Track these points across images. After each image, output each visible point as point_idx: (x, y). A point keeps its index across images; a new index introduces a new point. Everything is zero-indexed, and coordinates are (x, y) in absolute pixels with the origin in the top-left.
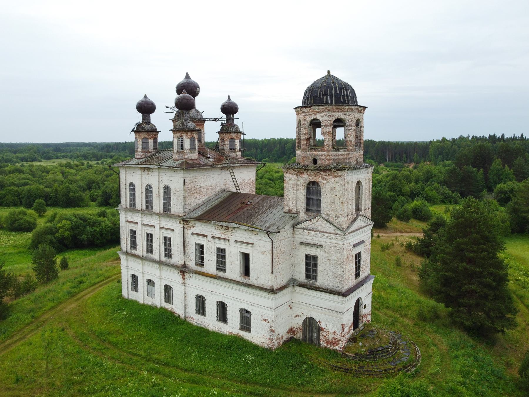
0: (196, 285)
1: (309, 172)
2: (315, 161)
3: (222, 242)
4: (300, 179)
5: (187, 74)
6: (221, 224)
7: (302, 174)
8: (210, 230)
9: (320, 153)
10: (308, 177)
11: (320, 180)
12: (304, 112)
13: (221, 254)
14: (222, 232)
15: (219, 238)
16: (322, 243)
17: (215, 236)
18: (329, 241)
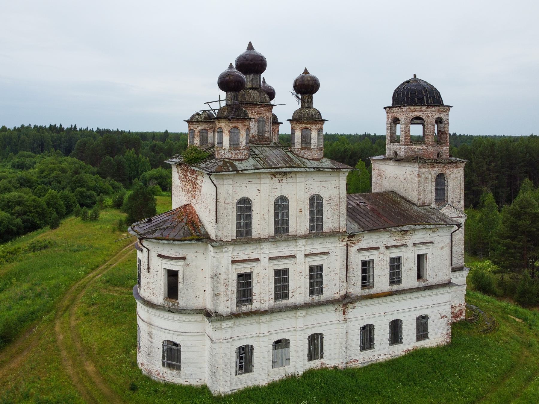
0: (362, 314)
3: (398, 250)
5: (250, 43)
6: (399, 229)
8: (381, 240)
12: (433, 111)
14: (397, 238)
15: (396, 246)
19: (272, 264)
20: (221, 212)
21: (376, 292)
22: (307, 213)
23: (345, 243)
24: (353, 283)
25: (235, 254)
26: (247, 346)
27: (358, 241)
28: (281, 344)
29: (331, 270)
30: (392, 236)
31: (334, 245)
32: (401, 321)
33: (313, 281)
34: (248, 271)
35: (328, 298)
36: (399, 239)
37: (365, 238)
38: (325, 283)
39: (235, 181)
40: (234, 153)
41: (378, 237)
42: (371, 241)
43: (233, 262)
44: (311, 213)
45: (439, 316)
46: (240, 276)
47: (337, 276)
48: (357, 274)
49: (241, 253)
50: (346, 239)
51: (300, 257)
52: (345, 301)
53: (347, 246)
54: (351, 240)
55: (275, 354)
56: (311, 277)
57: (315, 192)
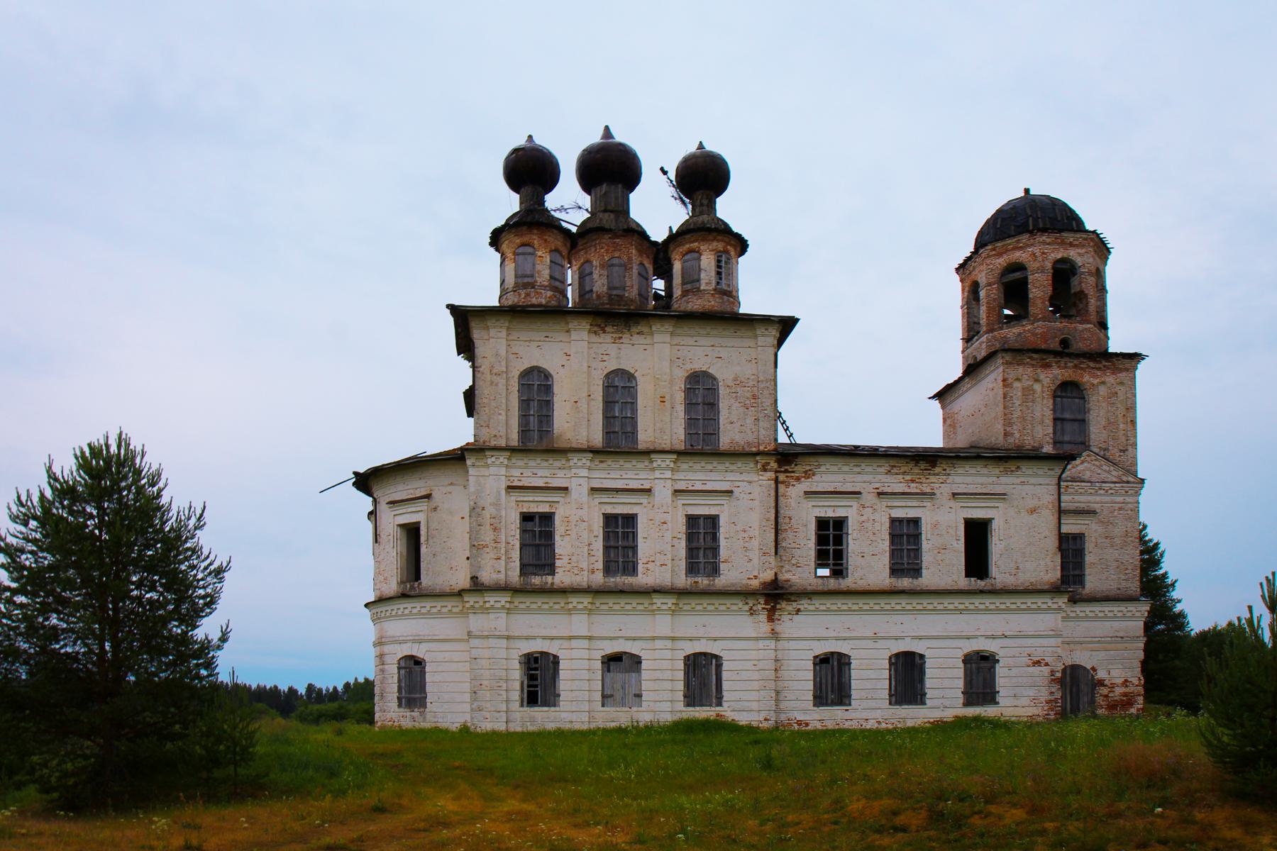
1: (1063, 361)
2: (1065, 343)
4: (1042, 377)
7: (1047, 366)
9: (1081, 327)
10: (1057, 373)
11: (1086, 378)
13: (906, 537)
14: (908, 478)
16: (1096, 507)
17: (886, 490)
18: (1108, 499)
19: (598, 501)
20: (486, 392)
21: (853, 587)
22: (680, 409)
23: (772, 475)
24: (794, 561)
25: (516, 473)
26: (544, 654)
27: (808, 475)
28: (619, 663)
29: (739, 528)
30: (895, 470)
31: (745, 477)
32: (922, 656)
33: (694, 545)
34: (544, 508)
35: (733, 585)
36: (913, 481)
37: (823, 468)
38: (723, 553)
39: (515, 335)
40: (523, 293)
41: (858, 469)
42: (840, 477)
43: (510, 488)
44: (690, 406)
45: (1026, 660)
46: (527, 518)
47: (755, 544)
48: (805, 543)
49: (528, 473)
50: (774, 465)
51: (663, 493)
52: (775, 595)
53: (777, 481)
54: (786, 471)
55: (608, 680)
56: (690, 537)
57: (699, 366)
